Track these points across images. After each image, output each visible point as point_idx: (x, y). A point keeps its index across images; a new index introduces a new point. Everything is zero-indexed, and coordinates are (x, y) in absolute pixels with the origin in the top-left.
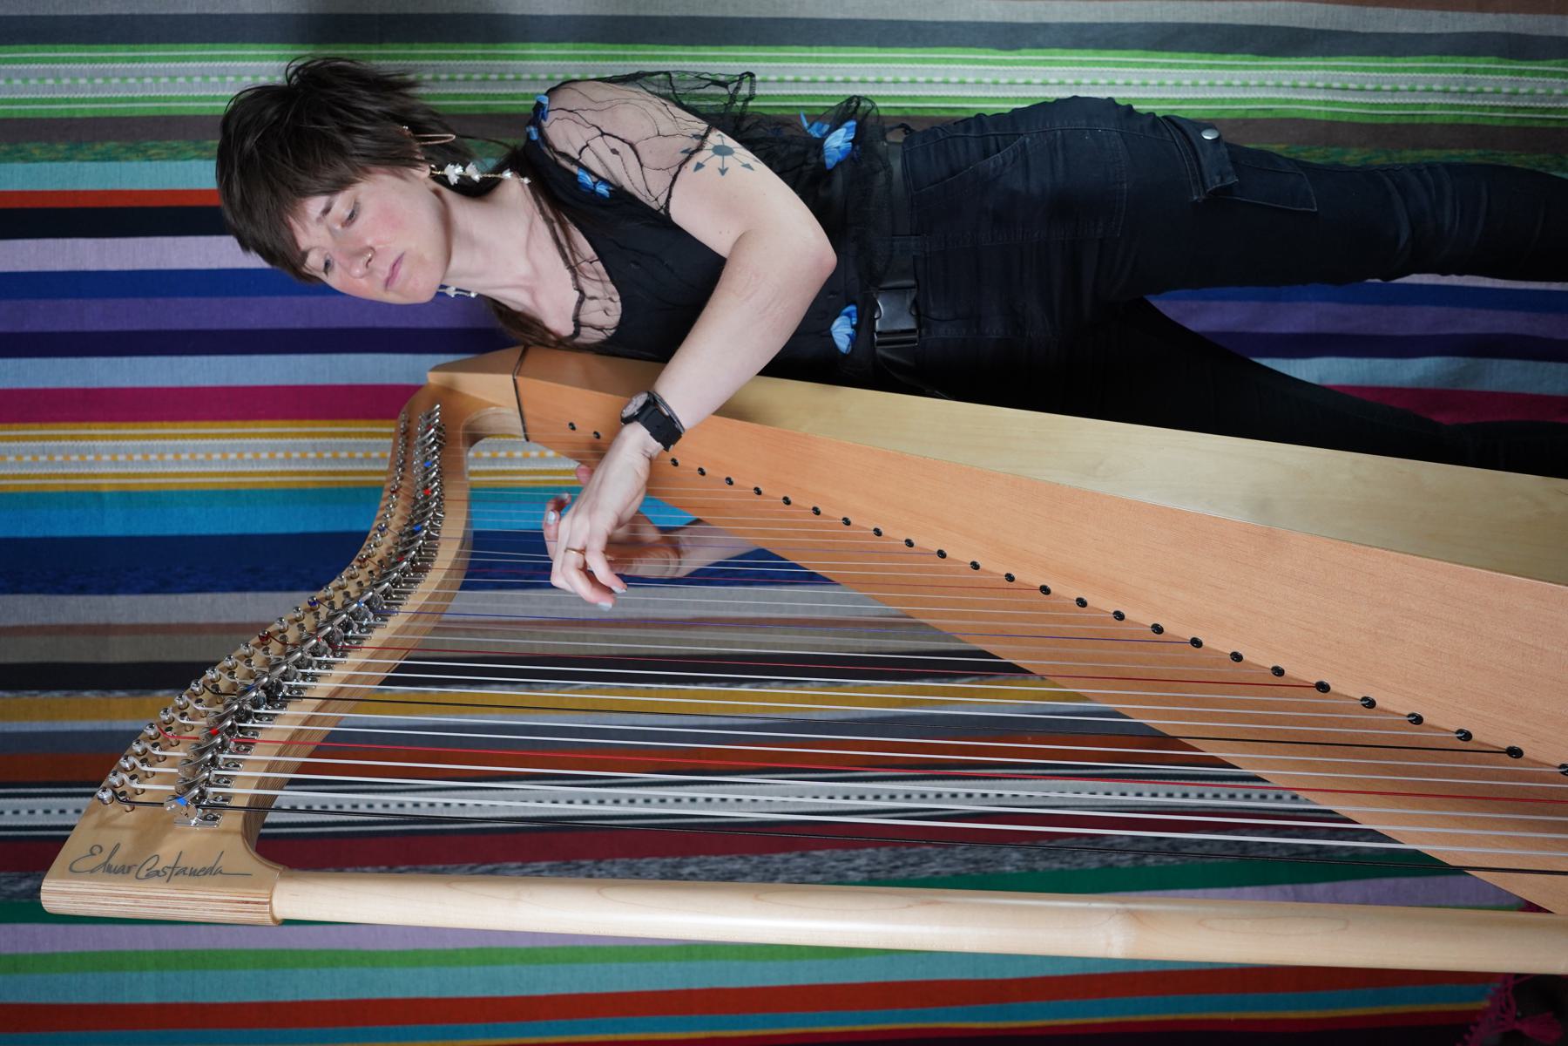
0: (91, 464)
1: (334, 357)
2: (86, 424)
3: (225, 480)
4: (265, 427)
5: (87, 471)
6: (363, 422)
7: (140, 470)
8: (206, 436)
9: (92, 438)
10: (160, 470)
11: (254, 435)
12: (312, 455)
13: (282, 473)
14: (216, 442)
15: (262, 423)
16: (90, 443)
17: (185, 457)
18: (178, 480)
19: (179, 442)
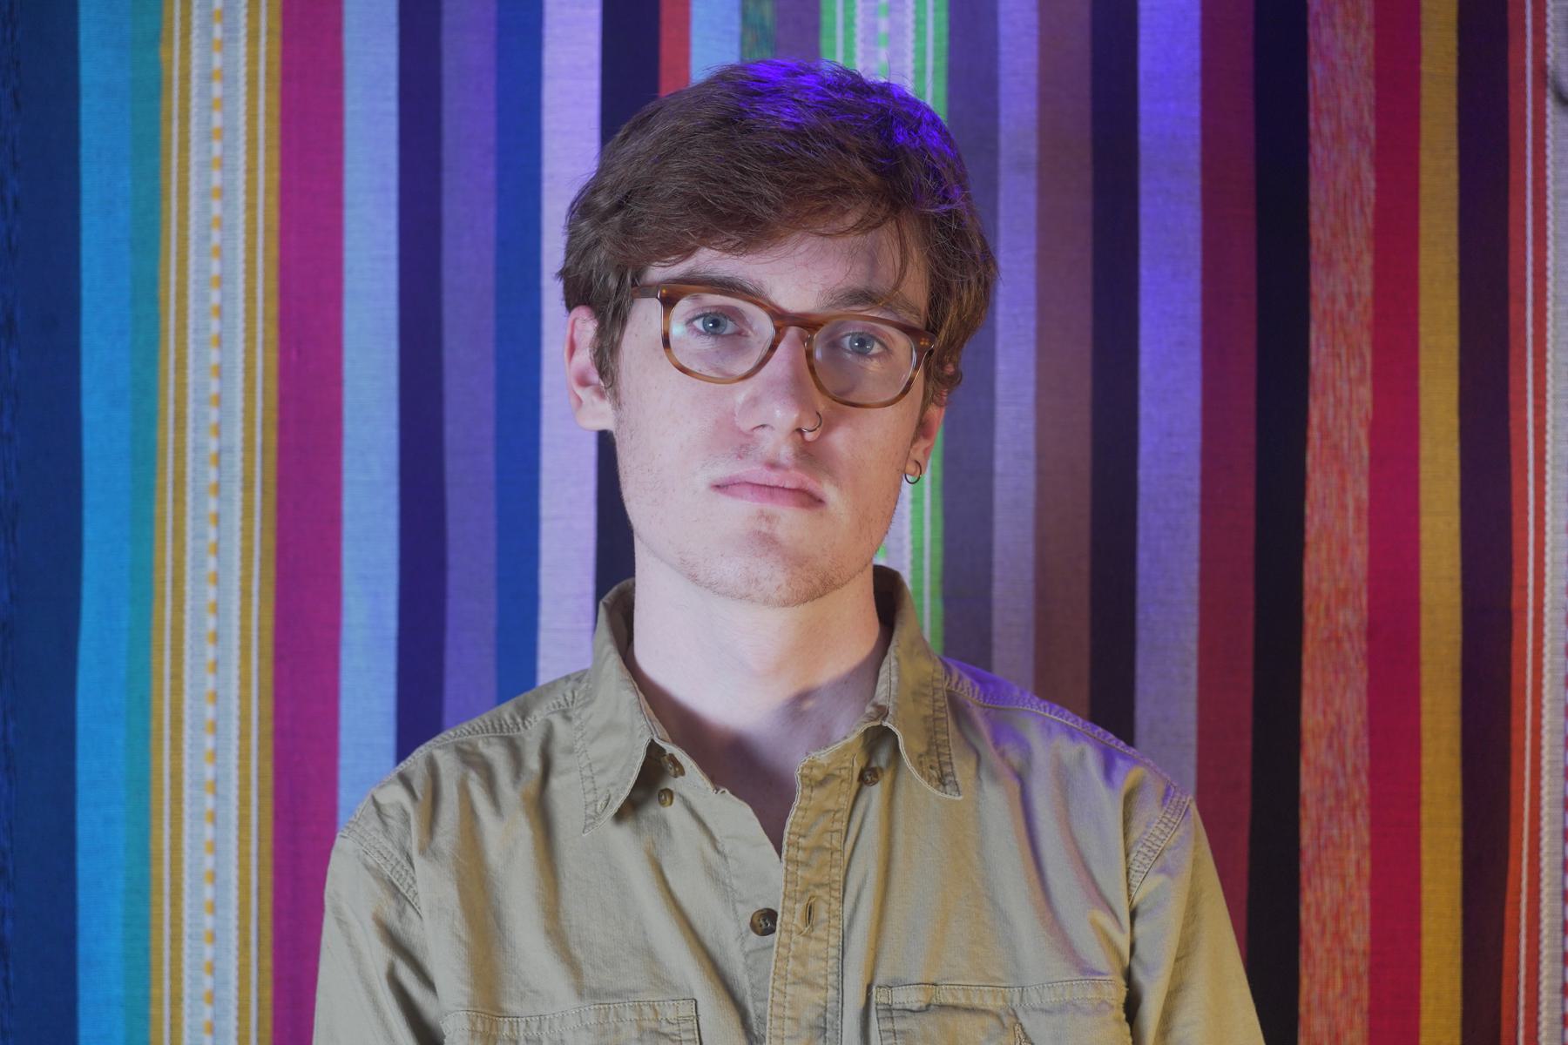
0: (206, 30)
1: (394, 490)
2: (277, 26)
3: (173, 277)
4: (265, 360)
5: (195, 22)
6: (272, 543)
7: (194, 120)
8: (251, 248)
9: (253, 37)
10: (194, 159)
11: (250, 338)
12: (213, 445)
13: (181, 386)
14: (241, 267)
15: (274, 356)
16: (243, 32)
17: (216, 208)
18: (174, 188)
19: (241, 198)
